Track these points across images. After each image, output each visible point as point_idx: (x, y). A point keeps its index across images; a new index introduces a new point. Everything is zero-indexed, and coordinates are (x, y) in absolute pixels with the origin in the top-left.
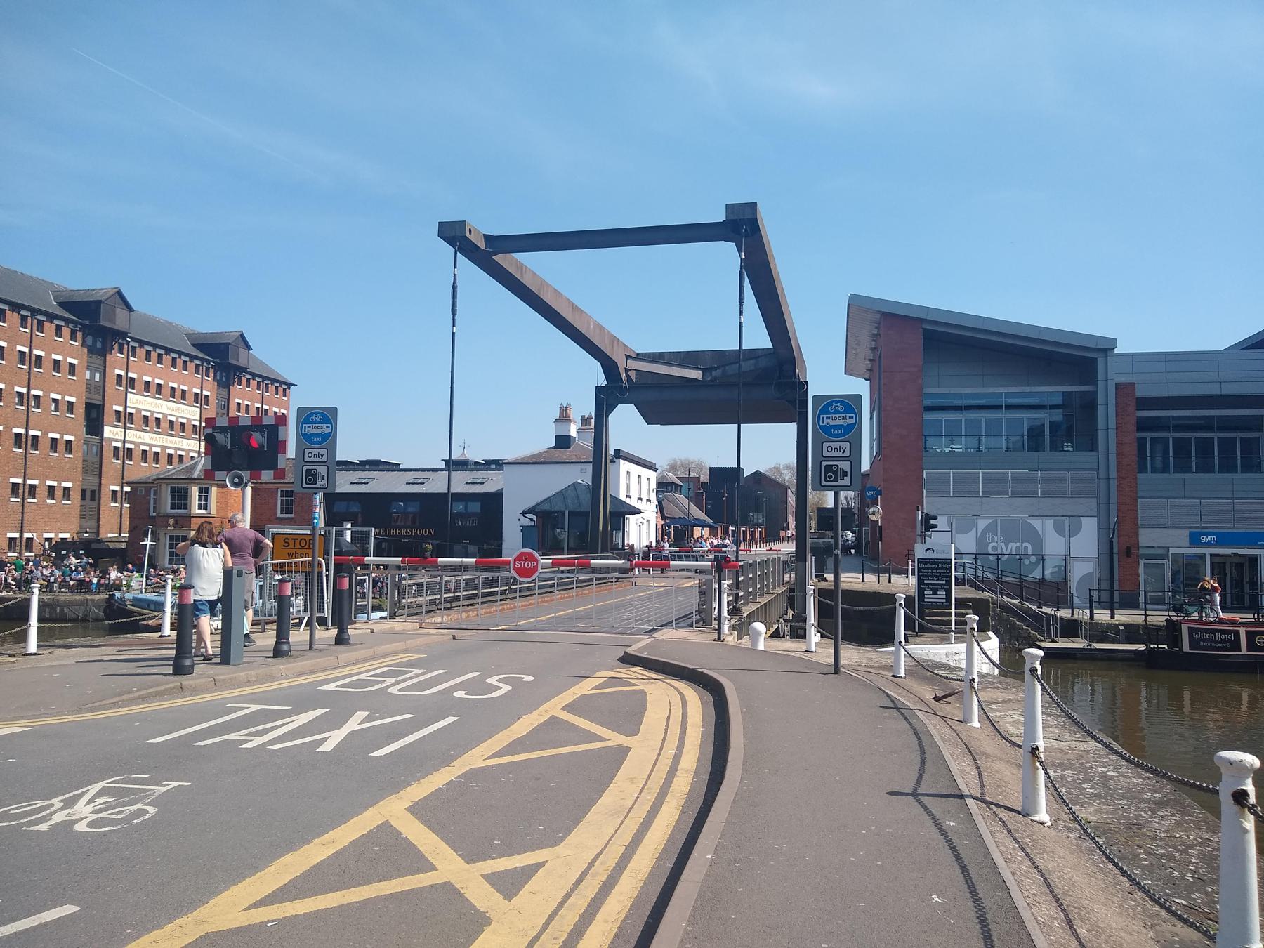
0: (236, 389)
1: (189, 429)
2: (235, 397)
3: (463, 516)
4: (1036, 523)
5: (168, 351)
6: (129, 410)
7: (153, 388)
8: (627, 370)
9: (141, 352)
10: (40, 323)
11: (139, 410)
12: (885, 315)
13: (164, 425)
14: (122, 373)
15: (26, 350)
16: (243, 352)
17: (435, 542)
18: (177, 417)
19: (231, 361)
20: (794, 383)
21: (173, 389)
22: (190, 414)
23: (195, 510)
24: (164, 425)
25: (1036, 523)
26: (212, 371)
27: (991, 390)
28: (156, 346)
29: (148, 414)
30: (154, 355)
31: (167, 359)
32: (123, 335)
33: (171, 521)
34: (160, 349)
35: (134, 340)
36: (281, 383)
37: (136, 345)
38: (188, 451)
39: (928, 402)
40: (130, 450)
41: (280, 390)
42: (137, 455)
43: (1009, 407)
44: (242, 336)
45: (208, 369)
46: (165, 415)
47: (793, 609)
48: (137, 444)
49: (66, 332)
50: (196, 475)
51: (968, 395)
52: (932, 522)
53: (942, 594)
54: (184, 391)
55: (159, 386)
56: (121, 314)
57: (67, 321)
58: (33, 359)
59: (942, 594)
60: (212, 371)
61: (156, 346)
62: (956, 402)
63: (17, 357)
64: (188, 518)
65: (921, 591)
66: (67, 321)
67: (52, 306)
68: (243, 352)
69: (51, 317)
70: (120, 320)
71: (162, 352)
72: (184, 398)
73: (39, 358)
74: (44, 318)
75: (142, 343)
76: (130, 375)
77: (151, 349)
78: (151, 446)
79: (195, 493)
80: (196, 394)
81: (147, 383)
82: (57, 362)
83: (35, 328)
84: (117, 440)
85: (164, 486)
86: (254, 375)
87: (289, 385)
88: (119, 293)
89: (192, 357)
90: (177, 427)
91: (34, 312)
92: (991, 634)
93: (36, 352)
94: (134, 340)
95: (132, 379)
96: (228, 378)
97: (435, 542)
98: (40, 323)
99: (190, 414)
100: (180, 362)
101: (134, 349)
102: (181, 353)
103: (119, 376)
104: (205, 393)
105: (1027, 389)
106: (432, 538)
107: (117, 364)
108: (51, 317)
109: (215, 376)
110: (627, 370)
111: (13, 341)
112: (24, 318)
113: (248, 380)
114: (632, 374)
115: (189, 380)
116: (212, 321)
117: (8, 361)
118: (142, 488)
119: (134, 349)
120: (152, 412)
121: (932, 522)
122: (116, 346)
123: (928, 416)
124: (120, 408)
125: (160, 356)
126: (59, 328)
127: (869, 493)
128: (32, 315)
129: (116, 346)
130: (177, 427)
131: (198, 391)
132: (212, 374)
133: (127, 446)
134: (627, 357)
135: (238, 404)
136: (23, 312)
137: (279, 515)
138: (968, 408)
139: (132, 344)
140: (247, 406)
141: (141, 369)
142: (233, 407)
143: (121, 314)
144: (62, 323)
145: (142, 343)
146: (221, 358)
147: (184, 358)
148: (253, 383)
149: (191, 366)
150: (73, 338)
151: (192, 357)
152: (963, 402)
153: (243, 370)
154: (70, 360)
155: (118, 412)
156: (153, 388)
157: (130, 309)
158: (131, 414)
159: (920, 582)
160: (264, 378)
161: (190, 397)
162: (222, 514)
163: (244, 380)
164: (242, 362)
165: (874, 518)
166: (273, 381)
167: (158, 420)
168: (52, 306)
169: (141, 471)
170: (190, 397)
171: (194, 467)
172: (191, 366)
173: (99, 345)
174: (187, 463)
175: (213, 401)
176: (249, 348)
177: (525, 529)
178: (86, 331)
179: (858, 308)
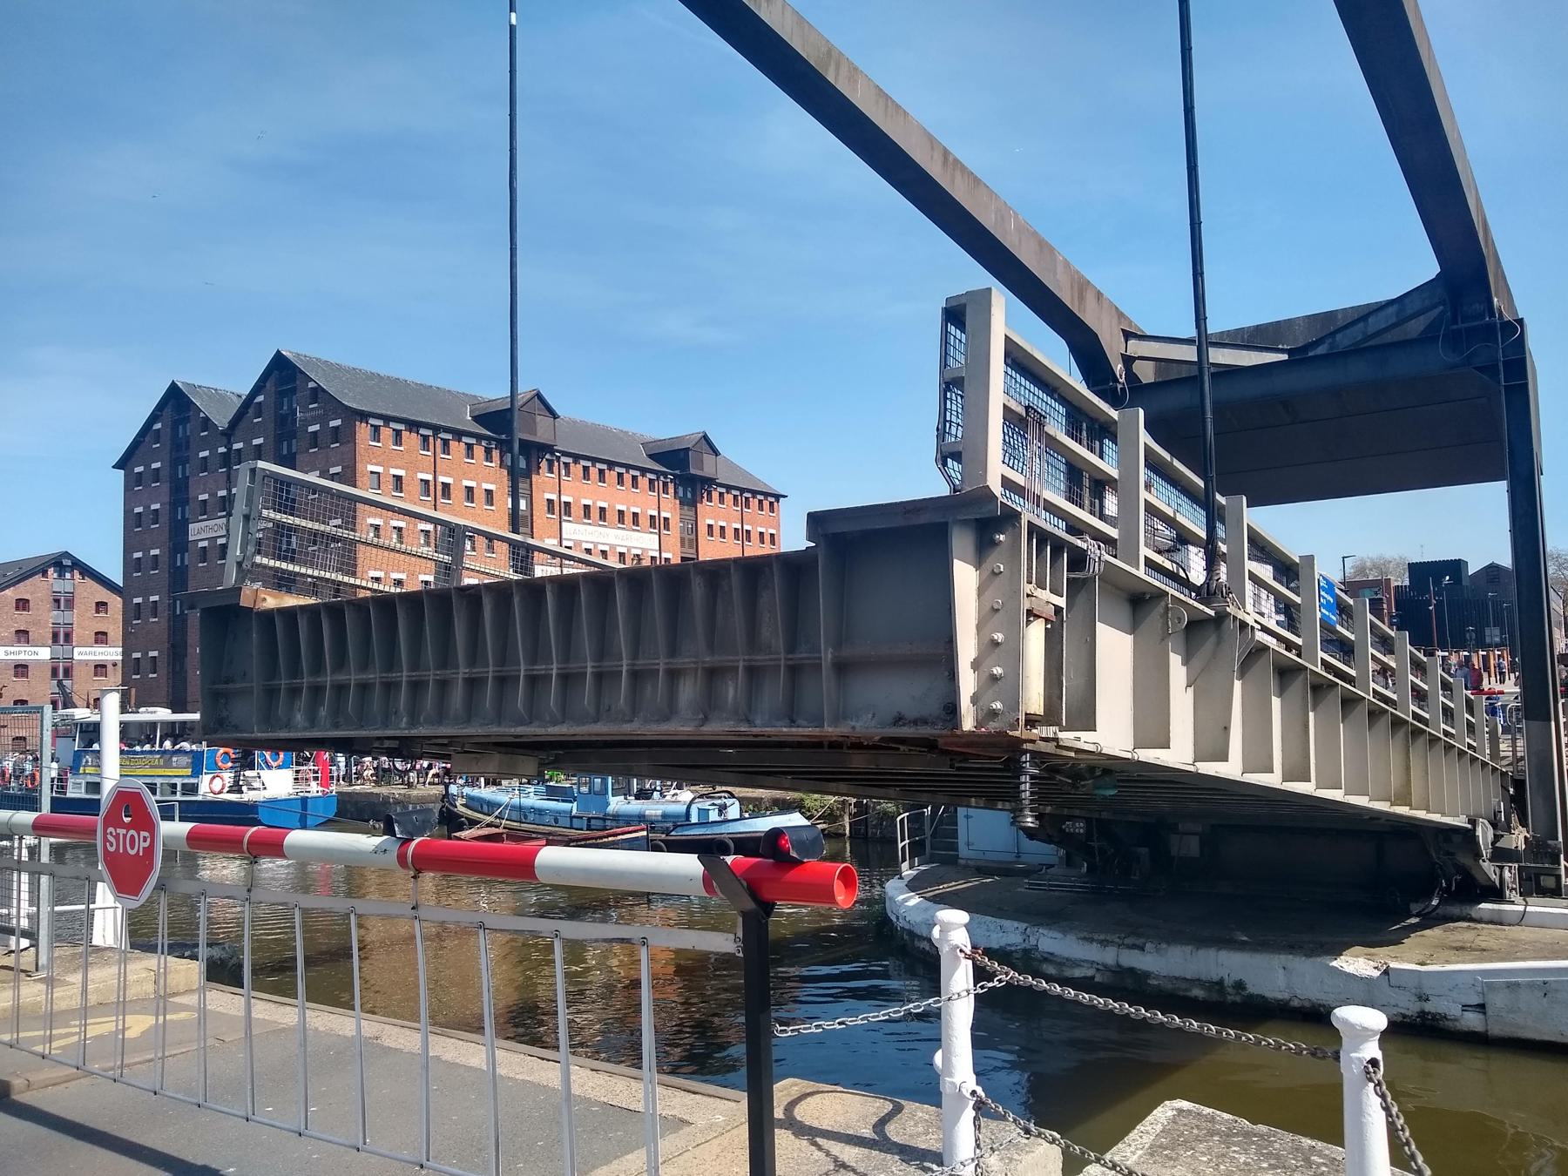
0: (704, 508)
2: (704, 517)
5: (611, 465)
7: (595, 514)
8: (1128, 361)
9: (577, 469)
10: (446, 442)
14: (554, 497)
15: (430, 477)
16: (708, 459)
18: (629, 549)
19: (692, 471)
20: (1491, 328)
21: (621, 513)
26: (496, 454)
28: (594, 460)
30: (594, 472)
31: (611, 476)
32: (549, 449)
34: (602, 462)
36: (766, 495)
37: (570, 460)
41: (766, 504)
44: (705, 437)
45: (665, 484)
46: (613, 547)
47: (1524, 823)
49: (479, 451)
55: (602, 510)
56: (543, 422)
57: (479, 437)
58: (439, 488)
61: (594, 460)
63: (463, 494)
66: (479, 437)
67: (466, 421)
68: (708, 459)
69: (459, 434)
70: (542, 432)
71: (604, 467)
73: (446, 486)
74: (449, 436)
75: (577, 458)
76: (564, 498)
77: (589, 464)
80: (652, 517)
81: (587, 507)
82: (470, 490)
83: (439, 450)
86: (729, 488)
87: (778, 497)
91: (437, 429)
93: (441, 479)
95: (567, 504)
96: (694, 494)
98: (446, 442)
101: (567, 465)
102: (628, 467)
103: (550, 502)
104: (664, 514)
107: (545, 485)
108: (459, 434)
110: (1128, 361)
111: (413, 467)
112: (425, 438)
113: (721, 494)
114: (1146, 373)
115: (643, 500)
116: (669, 425)
117: (409, 493)
119: (567, 465)
122: (544, 464)
125: (634, 478)
126: (470, 447)
128: (435, 433)
129: (544, 464)
131: (655, 513)
134: (1128, 335)
136: (422, 431)
139: (564, 459)
140: (722, 528)
141: (578, 490)
142: (703, 530)
143: (543, 422)
144: (473, 441)
145: (577, 458)
146: (682, 470)
147: (599, 466)
148: (729, 498)
150: (489, 458)
151: (644, 471)
153: (709, 482)
154: (486, 486)
157: (554, 416)
160: (742, 490)
161: (645, 522)
163: (715, 495)
164: (708, 471)
166: (754, 493)
168: (466, 421)
173: (523, 464)
175: (675, 524)
176: (716, 453)
178: (505, 447)
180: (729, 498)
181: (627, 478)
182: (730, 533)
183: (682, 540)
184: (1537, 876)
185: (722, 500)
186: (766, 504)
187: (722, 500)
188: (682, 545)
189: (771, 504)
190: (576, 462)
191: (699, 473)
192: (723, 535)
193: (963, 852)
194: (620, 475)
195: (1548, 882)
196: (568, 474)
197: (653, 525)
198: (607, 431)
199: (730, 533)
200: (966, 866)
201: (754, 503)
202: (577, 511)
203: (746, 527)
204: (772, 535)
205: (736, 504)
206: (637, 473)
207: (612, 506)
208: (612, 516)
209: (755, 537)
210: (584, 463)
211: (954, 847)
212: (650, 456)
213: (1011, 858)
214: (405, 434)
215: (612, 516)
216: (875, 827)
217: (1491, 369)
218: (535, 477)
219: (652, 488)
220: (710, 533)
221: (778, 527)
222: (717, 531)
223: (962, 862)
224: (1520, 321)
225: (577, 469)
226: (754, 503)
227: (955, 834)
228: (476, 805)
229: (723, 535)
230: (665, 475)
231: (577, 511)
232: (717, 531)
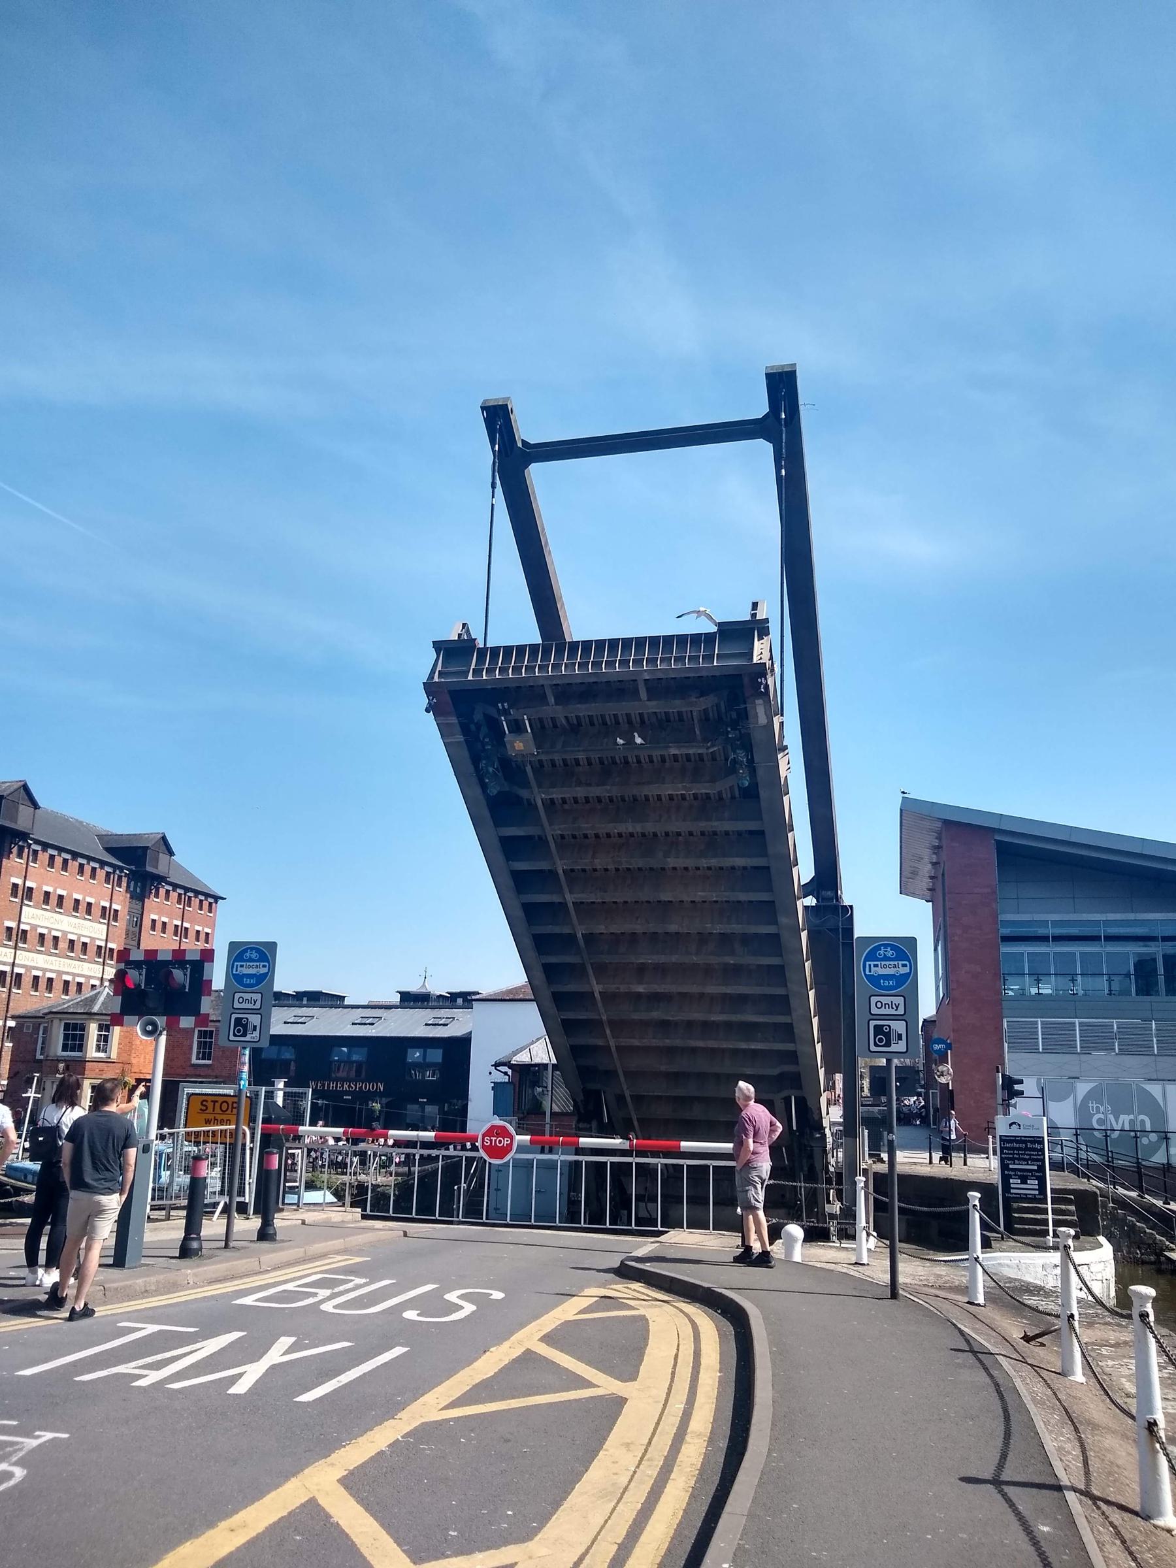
0: (152, 902)
1: (92, 950)
2: (150, 912)
3: (422, 1066)
4: (1155, 1089)
5: (75, 855)
6: (23, 927)
7: (53, 900)
9: (44, 857)
11: (34, 927)
12: (947, 823)
13: (63, 945)
14: (19, 881)
16: (163, 858)
18: (79, 936)
19: (149, 869)
21: (77, 901)
22: (94, 931)
23: (92, 1052)
24: (63, 945)
25: (1155, 1089)
26: (125, 880)
27: (1085, 917)
28: (61, 850)
29: (44, 931)
30: (58, 861)
31: (74, 865)
32: (24, 836)
33: (61, 1066)
34: (67, 853)
35: (37, 842)
36: (207, 895)
37: (38, 848)
38: (88, 977)
40: (19, 975)
41: (206, 904)
42: (27, 981)
43: (1110, 938)
44: (164, 839)
45: (120, 878)
46: (65, 933)
47: (840, 1199)
48: (29, 968)
50: (96, 1009)
51: (1055, 923)
52: (1017, 1087)
53: (1033, 1183)
54: (89, 904)
55: (61, 897)
56: (25, 811)
59: (1033, 1183)
60: (125, 880)
61: (61, 850)
62: (1041, 932)
64: (83, 1062)
65: (1005, 1179)
68: (163, 858)
70: (23, 819)
71: (68, 856)
72: (89, 912)
75: (45, 846)
76: (28, 884)
77: (55, 853)
78: (45, 970)
79: (93, 1030)
80: (104, 908)
81: (47, 894)
84: (4, 964)
85: (56, 1022)
86: (175, 886)
87: (217, 898)
88: (25, 787)
89: (103, 864)
90: (78, 947)
92: (1102, 1239)
94: (37, 842)
95: (30, 889)
96: (143, 888)
99: (94, 931)
100: (88, 869)
101: (35, 852)
102: (90, 859)
103: (15, 886)
104: (115, 906)
105: (1131, 916)
106: (381, 1095)
109: (128, 886)
113: (168, 892)
115: (97, 890)
116: (129, 822)
118: (29, 1023)
119: (35, 852)
120: (50, 929)
121: (1017, 1087)
122: (15, 850)
123: (1006, 949)
124: (13, 924)
125: (65, 861)
127: (937, 1047)
129: (15, 850)
130: (78, 947)
131: (107, 904)
132: (124, 884)
133: (17, 970)
135: (154, 921)
137: (194, 1061)
138: (1058, 939)
140: (164, 924)
142: (147, 923)
143: (25, 811)
145: (45, 846)
146: (138, 865)
148: (174, 895)
149: (101, 874)
151: (103, 864)
152: (1051, 932)
155: (9, 929)
156: (53, 900)
157: (35, 805)
158: (25, 932)
159: (1004, 1167)
160: (187, 890)
161: (96, 911)
162: (124, 1058)
163: (162, 892)
164: (161, 870)
165: (943, 1080)
166: (197, 893)
167: (56, 939)
169: (28, 1001)
170: (96, 911)
171: (93, 1000)
172: (101, 874)
174: (87, 993)
175: (124, 916)
176: (171, 853)
177: (497, 1087)
179: (915, 816)
180: (174, 895)
181: (58, 861)
182: (170, 929)
183: (127, 931)
185: (167, 898)
186: (206, 904)
187: (167, 898)
188: (127, 937)
189: (210, 904)
190: (74, 859)
191: (154, 871)
192: (164, 931)
194: (52, 857)
196: (35, 861)
197: (103, 916)
198: (65, 820)
199: (170, 929)
201: (195, 902)
202: (38, 896)
203: (186, 925)
204: (207, 934)
205: (179, 902)
206: (96, 865)
207: (98, 903)
208: (69, 904)
209: (192, 934)
210: (81, 860)
212: (109, 850)
214: (40, 854)
215: (69, 904)
217: (835, 930)
218: (5, 862)
219: (107, 881)
220: (153, 928)
221: (213, 927)
222: (159, 926)
224: (851, 907)
225: (44, 857)
226: (195, 902)
228: (13, 1173)
229: (164, 931)
230: (121, 869)
231: (38, 896)
232: (159, 926)
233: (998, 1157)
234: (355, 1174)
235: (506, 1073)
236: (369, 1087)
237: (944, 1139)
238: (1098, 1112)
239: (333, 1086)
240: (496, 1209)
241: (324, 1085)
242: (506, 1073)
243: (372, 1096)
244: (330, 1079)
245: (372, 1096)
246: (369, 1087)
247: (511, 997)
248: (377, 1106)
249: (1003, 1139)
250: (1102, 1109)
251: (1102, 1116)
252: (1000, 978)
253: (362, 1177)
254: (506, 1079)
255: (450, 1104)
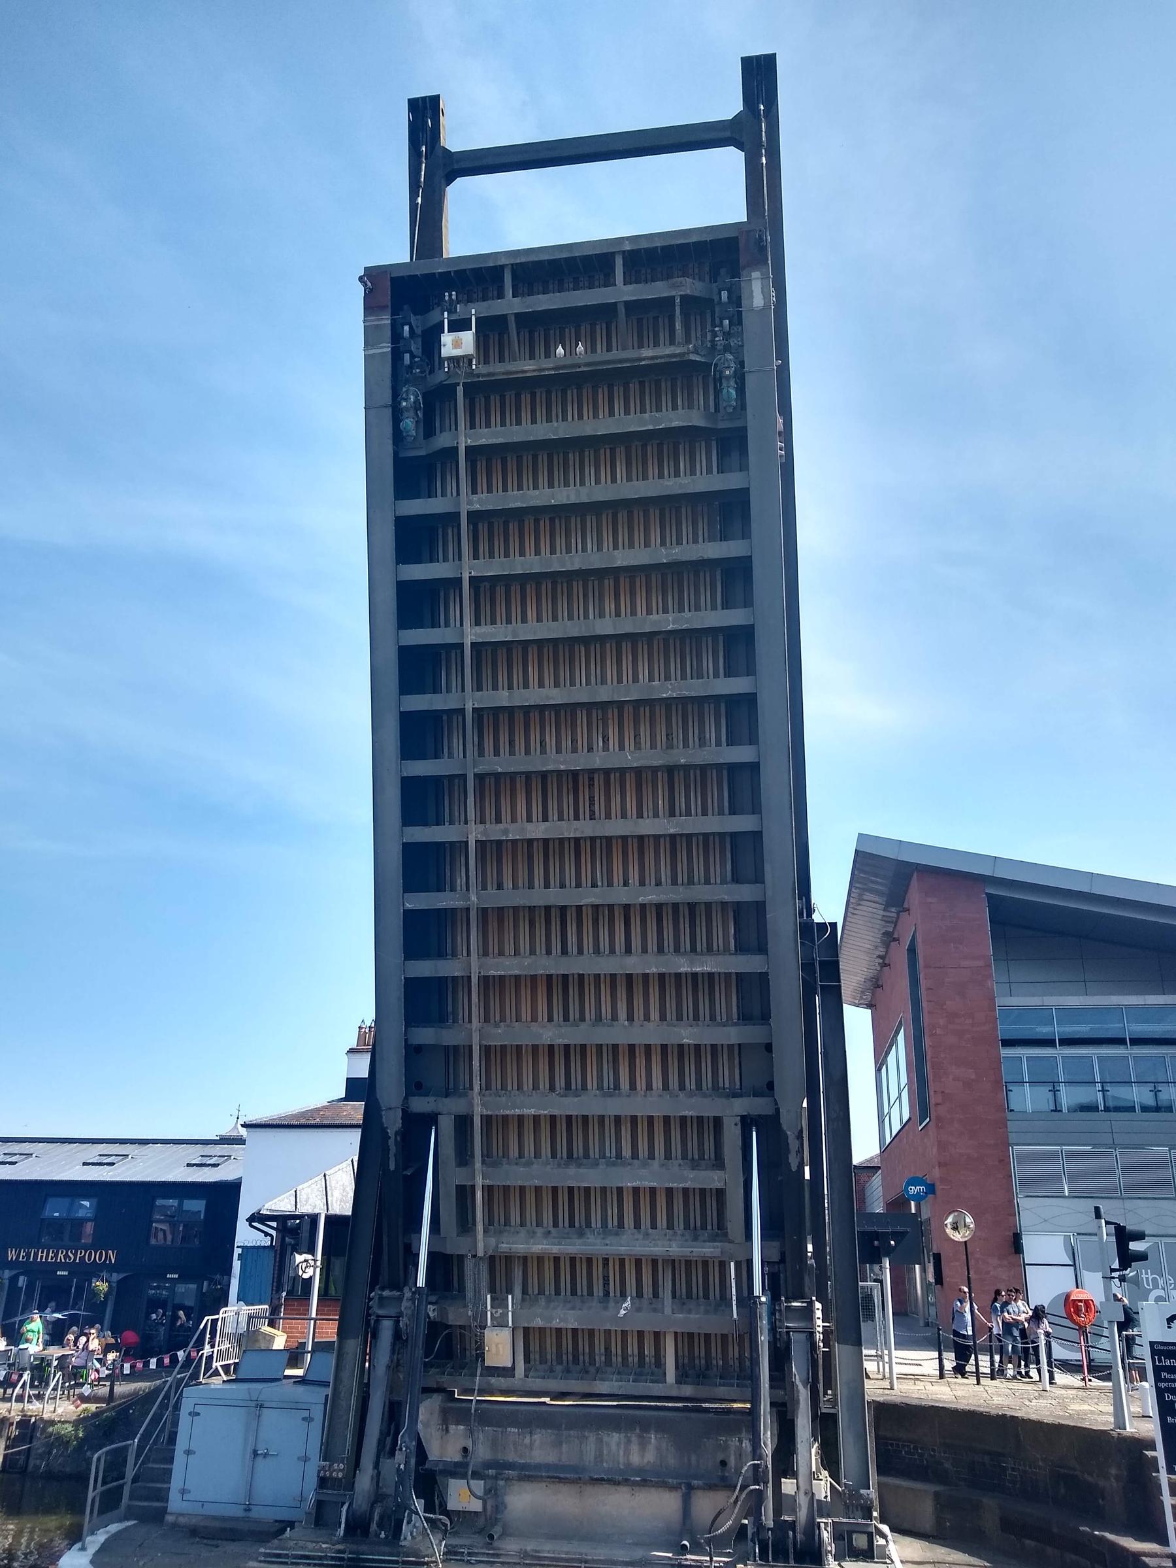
17: (115, 1277)
39: (1004, 1029)
43: (1136, 1042)
51: (1068, 1014)
52: (1134, 1246)
62: (1043, 1030)
97: (115, 1277)
106: (111, 1268)
121: (1134, 1246)
123: (1006, 1052)
127: (913, 1190)
152: (1058, 1030)
165: (957, 1237)
184: (850, 1533)
193: (175, 1503)
195: (860, 1541)
200: (174, 1526)
211: (163, 1496)
213: (238, 1512)
216: (41, 1457)
223: (169, 1518)
227: (167, 1475)
233: (1148, 1386)
234: (20, 1399)
235: (266, 1234)
236: (95, 1256)
237: (956, 1334)
238: (1156, 1286)
239: (42, 1255)
240: (183, 1491)
241: (28, 1255)
242: (266, 1234)
243: (95, 1270)
244: (40, 1246)
245: (95, 1270)
246: (95, 1256)
247: (303, 1121)
248: (102, 1286)
249: (1157, 1349)
250: (1161, 1282)
251: (1161, 1293)
252: (1001, 1087)
253: (34, 1407)
254: (266, 1242)
255: (211, 1281)
